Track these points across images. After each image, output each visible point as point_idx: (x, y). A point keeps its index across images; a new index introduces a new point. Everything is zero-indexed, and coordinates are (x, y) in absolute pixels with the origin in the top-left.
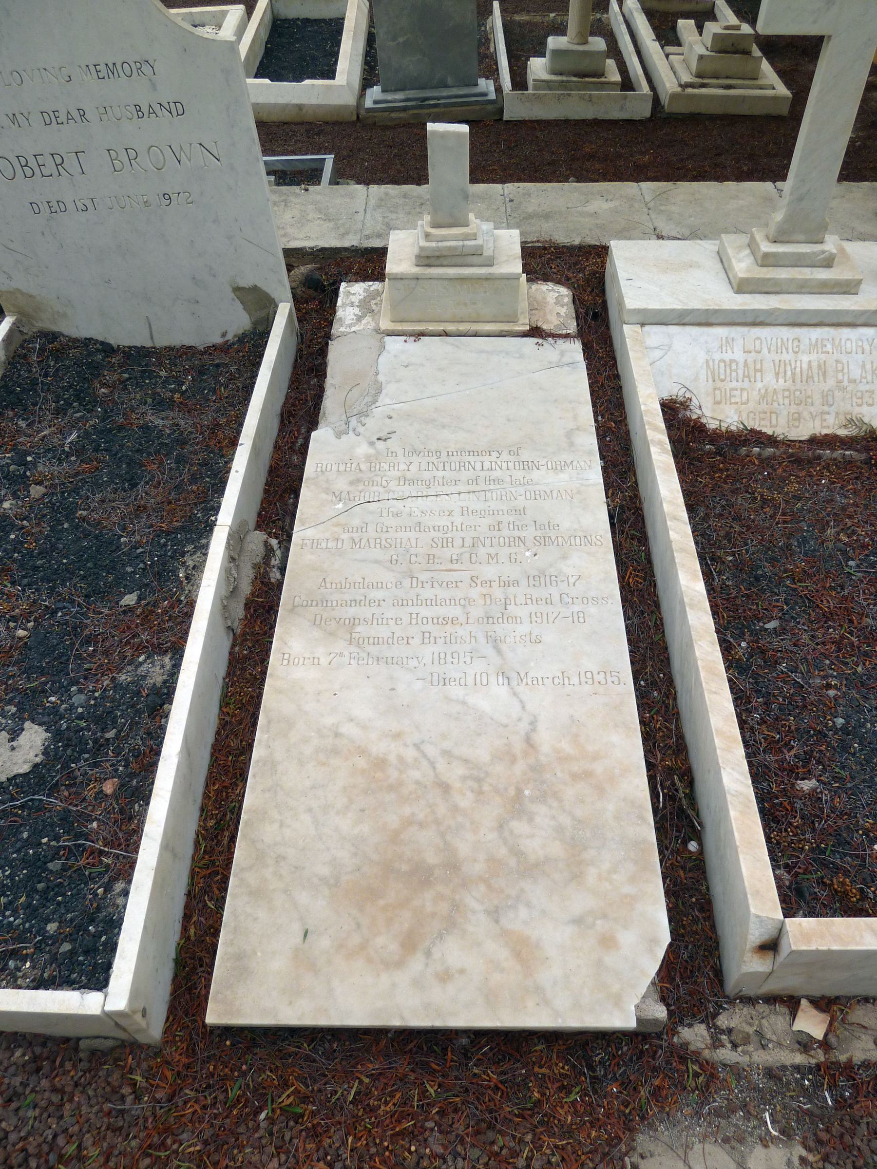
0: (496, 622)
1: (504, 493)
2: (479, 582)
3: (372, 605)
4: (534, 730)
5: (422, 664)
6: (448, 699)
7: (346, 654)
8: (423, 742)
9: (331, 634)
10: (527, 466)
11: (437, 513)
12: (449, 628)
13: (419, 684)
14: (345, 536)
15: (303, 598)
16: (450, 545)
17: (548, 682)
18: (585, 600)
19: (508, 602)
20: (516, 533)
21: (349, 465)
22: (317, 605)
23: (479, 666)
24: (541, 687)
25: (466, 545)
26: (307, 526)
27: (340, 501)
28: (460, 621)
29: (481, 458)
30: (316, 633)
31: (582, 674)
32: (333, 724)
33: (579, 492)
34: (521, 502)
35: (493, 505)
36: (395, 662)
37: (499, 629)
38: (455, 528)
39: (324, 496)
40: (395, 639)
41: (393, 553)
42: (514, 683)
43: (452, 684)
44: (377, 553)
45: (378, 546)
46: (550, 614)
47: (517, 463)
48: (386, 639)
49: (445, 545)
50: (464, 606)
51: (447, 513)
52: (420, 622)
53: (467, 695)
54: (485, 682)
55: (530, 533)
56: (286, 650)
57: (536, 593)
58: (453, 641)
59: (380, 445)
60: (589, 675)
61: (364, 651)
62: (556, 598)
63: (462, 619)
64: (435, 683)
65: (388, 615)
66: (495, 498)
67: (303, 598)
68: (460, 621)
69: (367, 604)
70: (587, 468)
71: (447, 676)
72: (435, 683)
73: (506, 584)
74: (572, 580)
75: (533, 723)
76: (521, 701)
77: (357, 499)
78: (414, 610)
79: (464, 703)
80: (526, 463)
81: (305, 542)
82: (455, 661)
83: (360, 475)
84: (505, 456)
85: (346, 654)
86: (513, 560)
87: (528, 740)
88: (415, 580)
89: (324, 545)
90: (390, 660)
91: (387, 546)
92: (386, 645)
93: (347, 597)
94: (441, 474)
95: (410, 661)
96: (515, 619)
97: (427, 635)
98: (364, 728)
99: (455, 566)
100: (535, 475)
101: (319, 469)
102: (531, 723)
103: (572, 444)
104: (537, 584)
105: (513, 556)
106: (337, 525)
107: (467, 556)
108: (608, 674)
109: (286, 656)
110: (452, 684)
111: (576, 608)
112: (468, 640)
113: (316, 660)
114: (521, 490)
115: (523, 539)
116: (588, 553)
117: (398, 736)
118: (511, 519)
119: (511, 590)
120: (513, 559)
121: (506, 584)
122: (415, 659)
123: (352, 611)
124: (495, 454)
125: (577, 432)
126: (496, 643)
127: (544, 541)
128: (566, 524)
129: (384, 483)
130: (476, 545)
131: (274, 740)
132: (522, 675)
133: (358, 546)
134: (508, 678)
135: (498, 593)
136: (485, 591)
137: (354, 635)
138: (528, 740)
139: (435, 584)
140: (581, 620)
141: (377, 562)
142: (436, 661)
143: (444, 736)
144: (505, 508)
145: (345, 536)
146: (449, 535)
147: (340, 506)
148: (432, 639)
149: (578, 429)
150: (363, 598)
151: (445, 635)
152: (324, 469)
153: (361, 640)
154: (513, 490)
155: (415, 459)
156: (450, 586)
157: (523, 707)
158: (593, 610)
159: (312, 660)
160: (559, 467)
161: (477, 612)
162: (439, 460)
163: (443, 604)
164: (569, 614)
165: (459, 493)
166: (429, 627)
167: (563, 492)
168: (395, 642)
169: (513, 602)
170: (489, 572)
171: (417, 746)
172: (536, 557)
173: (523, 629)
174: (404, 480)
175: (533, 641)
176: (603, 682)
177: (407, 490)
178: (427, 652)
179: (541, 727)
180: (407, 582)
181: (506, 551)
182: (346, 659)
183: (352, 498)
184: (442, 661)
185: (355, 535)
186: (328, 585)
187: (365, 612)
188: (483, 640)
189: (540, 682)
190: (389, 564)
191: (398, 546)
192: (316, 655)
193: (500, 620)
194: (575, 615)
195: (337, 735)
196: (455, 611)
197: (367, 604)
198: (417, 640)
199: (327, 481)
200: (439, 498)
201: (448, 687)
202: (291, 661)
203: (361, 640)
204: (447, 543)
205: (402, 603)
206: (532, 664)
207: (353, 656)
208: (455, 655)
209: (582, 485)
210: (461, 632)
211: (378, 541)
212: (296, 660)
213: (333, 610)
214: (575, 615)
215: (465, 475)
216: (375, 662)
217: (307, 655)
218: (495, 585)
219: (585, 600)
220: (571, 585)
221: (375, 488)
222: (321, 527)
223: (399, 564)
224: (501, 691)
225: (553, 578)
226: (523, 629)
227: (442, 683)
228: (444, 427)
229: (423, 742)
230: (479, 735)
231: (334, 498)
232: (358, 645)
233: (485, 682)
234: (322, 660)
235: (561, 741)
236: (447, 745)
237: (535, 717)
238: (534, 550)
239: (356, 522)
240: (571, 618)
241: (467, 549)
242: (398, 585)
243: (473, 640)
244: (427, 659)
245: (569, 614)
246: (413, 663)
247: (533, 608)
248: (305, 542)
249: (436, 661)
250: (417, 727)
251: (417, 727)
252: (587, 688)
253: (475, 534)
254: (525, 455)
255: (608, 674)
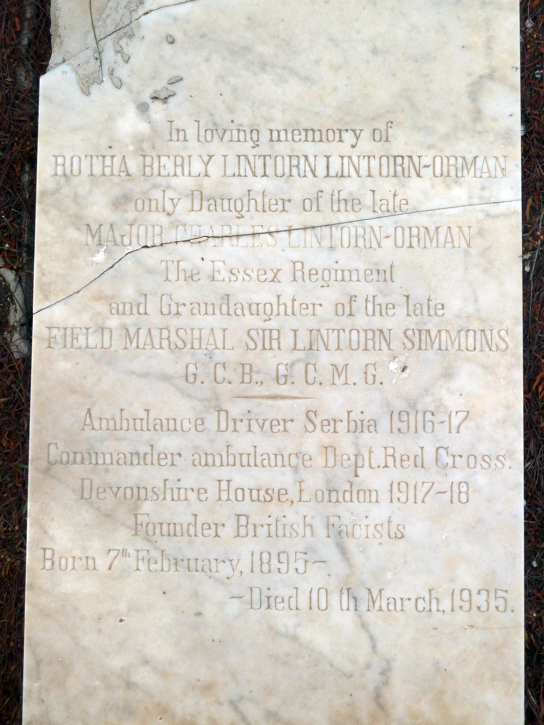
0: (341, 499)
1: (360, 231)
2: (317, 422)
3: (163, 462)
4: (386, 683)
5: (237, 573)
6: (273, 631)
7: (131, 551)
8: (241, 698)
9: (108, 516)
10: (403, 167)
11: (254, 275)
12: (273, 508)
13: (234, 606)
14: (113, 322)
15: (62, 447)
16: (275, 344)
17: (409, 606)
18: (472, 459)
19: (360, 464)
20: (377, 322)
21: (108, 161)
22: (82, 462)
23: (315, 578)
24: (399, 615)
25: (300, 346)
26: (53, 299)
27: (100, 244)
28: (290, 496)
29: (324, 147)
30: (87, 515)
31: (457, 592)
32: (122, 669)
33: (481, 233)
34: (387, 254)
35: (346, 258)
36: (199, 568)
37: (347, 512)
38: (282, 308)
39: (73, 234)
40: (199, 527)
41: (188, 359)
42: (363, 607)
43: (280, 606)
44: (163, 360)
45: (165, 343)
46: (419, 485)
47: (384, 160)
48: (185, 526)
49: (267, 346)
50: (296, 469)
51: (270, 275)
52: (232, 497)
53: (299, 625)
54: (323, 605)
55: (397, 322)
56: (47, 544)
57: (405, 445)
58: (280, 533)
59: (157, 110)
60: (466, 595)
61: (156, 548)
62: (429, 455)
63: (293, 493)
64: (256, 605)
65: (187, 483)
66: (346, 244)
67: (61, 447)
68: (290, 496)
69: (155, 461)
70: (499, 174)
71: (273, 593)
72: (256, 605)
73: (359, 427)
74: (455, 421)
75: (385, 672)
76: (371, 638)
77: (126, 241)
78: (224, 473)
79: (295, 638)
80: (399, 160)
81: (55, 332)
82: (283, 568)
83: (129, 185)
84: (366, 145)
85: (131, 551)
86: (370, 379)
87: (378, 698)
88: (223, 414)
89: (82, 340)
90: (192, 564)
91: (180, 344)
92: (186, 538)
93: (126, 447)
94: (259, 184)
95: (221, 566)
96: (368, 495)
97: (243, 520)
98: (164, 674)
99: (284, 390)
100: (415, 189)
101: (60, 170)
102: (383, 673)
103: (477, 115)
104: (404, 426)
105: (371, 369)
106: (99, 298)
107: (301, 367)
108: (492, 595)
109: (49, 554)
110: (280, 606)
111: (458, 476)
112: (301, 532)
113: (90, 562)
114: (388, 223)
115: (386, 333)
116: (484, 367)
117: (208, 688)
118: (370, 290)
119: (366, 438)
120: (371, 379)
121: (359, 427)
122: (228, 563)
123: (134, 474)
124: (348, 137)
125: (489, 84)
126: (339, 535)
127: (419, 339)
128: (455, 304)
129: (169, 207)
130: (315, 347)
131: (47, 691)
132: (375, 593)
133: (134, 344)
134: (355, 599)
135: (346, 444)
136: (326, 439)
137: (140, 518)
138: (378, 698)
139: (255, 427)
140: (463, 497)
141: (165, 378)
142: (257, 568)
143: (269, 691)
144: (362, 266)
145: (113, 322)
146: (272, 324)
147: (100, 257)
148: (251, 527)
149: (491, 77)
150: (149, 450)
151: (269, 521)
152: (68, 172)
153: (151, 527)
154: (375, 223)
155: (217, 147)
156: (275, 429)
157: (374, 647)
158: (481, 479)
159: (84, 560)
160: (453, 173)
161: (314, 481)
162: (256, 151)
163: (266, 462)
164: (446, 487)
165: (289, 231)
166: (246, 507)
167: (455, 230)
168: (199, 533)
169: (367, 464)
170: (334, 401)
171: (234, 704)
172: (405, 374)
173: (380, 512)
174: (200, 198)
175: (392, 535)
176: (484, 607)
177: (205, 221)
178: (246, 549)
179: (396, 678)
180: (211, 420)
181: (361, 359)
182: (131, 561)
183: (118, 239)
184: (265, 568)
185: (129, 320)
186: (96, 424)
187: (153, 476)
188: (321, 531)
189: (399, 607)
190: (182, 383)
191: (196, 346)
192: (90, 554)
193: (348, 495)
194: (455, 488)
195: (130, 685)
196: (281, 478)
197: (155, 461)
198: (228, 532)
199: (76, 198)
200: (258, 240)
201: (273, 611)
202: (57, 563)
203: (151, 527)
204: (268, 340)
205: (204, 460)
206: (389, 576)
207: (141, 555)
208: (283, 558)
209: (488, 215)
210: (292, 516)
211: (165, 334)
212: (63, 561)
213: (107, 471)
214: (455, 488)
215: (301, 188)
216: (173, 569)
217: (77, 553)
218: (342, 427)
219: (472, 459)
220: (454, 430)
221: (154, 217)
222: (75, 301)
223: (198, 382)
224: (343, 619)
225: (429, 416)
226: (380, 512)
227: (265, 605)
228: (264, 66)
229: (241, 698)
230: (314, 689)
231: (90, 239)
232: (147, 538)
233: (323, 605)
234: (99, 562)
235: (420, 700)
236: (273, 703)
237: (388, 662)
238: (402, 358)
239: (129, 292)
240: (448, 494)
241: (300, 355)
242: (199, 424)
243: (308, 530)
244: (244, 565)
245: (446, 487)
246: (225, 570)
247: (395, 474)
248: (55, 332)
249: (257, 568)
250: (233, 675)
251: (233, 675)
252: (461, 617)
253: (312, 323)
254: (401, 142)
255: (492, 595)
